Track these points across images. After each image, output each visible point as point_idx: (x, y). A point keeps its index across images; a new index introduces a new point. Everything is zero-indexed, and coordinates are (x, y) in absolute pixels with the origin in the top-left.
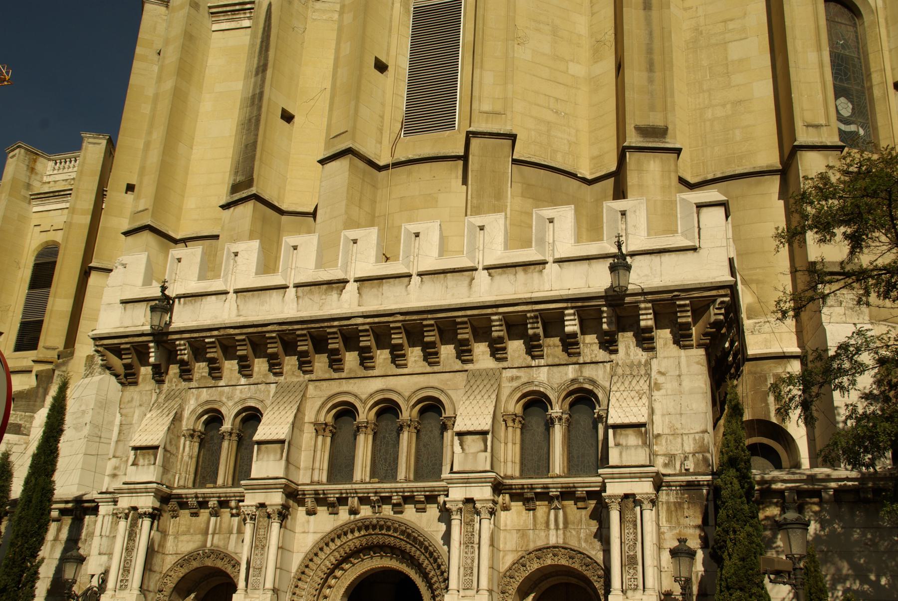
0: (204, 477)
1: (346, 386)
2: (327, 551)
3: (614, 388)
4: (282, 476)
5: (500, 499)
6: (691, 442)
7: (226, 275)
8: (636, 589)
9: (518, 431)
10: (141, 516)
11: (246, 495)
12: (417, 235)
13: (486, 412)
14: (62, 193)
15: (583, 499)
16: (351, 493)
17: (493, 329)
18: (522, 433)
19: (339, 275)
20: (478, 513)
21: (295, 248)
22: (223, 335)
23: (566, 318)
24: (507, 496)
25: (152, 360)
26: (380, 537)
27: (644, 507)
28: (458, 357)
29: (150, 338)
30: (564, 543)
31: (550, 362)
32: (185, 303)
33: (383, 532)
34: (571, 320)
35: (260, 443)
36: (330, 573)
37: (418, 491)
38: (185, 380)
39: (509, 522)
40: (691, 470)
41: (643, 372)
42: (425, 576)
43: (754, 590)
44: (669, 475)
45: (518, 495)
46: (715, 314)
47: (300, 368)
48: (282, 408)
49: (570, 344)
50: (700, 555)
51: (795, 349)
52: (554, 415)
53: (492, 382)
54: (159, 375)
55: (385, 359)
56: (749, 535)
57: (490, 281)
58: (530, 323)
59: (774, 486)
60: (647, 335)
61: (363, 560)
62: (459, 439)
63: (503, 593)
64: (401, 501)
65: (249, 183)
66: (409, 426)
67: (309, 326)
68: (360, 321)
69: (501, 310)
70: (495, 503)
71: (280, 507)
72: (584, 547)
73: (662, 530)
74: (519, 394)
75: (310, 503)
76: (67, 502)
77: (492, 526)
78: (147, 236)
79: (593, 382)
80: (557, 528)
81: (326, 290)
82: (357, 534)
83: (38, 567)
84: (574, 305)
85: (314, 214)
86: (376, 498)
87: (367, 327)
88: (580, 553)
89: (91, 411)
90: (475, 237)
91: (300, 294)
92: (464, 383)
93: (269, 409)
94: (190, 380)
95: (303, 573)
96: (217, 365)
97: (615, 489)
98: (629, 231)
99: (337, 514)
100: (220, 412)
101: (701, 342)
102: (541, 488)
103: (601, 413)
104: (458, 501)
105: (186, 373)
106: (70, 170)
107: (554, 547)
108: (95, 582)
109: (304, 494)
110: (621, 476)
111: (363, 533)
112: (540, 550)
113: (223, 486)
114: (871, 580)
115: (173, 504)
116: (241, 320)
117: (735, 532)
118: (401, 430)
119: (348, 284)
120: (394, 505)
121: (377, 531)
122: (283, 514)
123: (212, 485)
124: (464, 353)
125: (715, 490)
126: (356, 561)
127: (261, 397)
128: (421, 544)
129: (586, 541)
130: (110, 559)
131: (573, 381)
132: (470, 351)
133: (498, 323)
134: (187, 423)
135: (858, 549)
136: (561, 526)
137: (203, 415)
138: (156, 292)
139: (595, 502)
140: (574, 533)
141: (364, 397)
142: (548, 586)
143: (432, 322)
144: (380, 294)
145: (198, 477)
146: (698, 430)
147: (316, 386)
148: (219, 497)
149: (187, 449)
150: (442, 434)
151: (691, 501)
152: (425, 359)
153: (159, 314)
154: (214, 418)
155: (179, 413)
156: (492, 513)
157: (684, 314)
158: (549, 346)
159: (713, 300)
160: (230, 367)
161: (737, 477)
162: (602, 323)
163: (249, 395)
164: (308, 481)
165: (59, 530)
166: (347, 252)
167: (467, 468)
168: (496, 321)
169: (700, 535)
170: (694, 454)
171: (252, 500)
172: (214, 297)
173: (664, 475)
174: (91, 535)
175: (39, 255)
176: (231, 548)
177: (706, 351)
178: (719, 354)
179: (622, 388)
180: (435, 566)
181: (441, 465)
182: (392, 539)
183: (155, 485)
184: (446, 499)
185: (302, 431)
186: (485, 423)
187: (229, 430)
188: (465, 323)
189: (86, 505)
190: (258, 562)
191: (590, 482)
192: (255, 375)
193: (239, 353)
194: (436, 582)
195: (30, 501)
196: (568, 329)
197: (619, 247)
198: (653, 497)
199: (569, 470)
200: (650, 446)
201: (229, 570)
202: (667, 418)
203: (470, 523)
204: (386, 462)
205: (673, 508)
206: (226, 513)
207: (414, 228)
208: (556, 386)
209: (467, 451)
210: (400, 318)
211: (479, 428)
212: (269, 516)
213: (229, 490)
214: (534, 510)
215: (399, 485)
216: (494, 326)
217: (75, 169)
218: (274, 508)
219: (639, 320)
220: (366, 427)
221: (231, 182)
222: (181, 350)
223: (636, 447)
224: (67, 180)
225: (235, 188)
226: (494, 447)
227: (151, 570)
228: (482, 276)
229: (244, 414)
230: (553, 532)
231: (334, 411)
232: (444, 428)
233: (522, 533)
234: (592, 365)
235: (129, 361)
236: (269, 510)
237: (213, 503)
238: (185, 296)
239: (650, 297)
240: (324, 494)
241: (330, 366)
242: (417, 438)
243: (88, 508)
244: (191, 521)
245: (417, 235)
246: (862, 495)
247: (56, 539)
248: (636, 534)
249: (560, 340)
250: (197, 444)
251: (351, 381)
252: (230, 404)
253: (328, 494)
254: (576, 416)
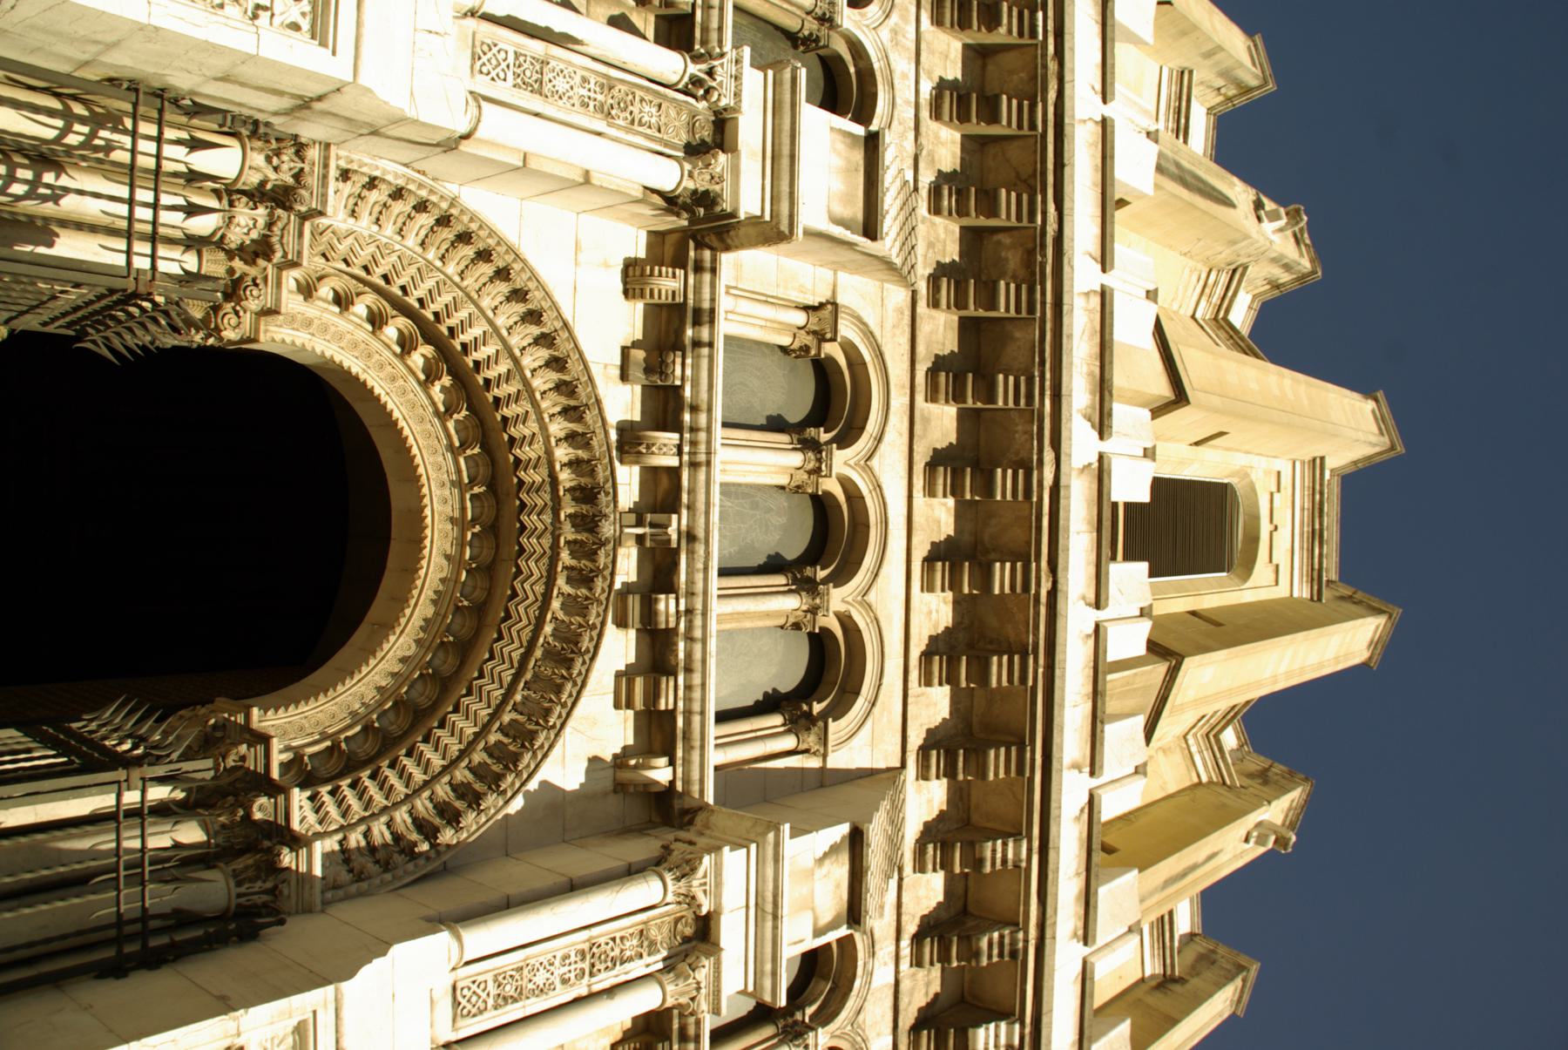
16: (693, 443)
22: (1045, 67)
31: (905, 985)
33: (565, 557)
34: (997, 1036)
37: (688, 688)
57: (1074, 816)
58: (1002, 937)
71: (727, 206)
75: (668, 284)
84: (1027, 1039)
86: (674, 537)
99: (624, 377)
104: (718, 896)
109: (698, 268)
111: (565, 477)
119: (1096, 434)
121: (568, 533)
133: (1010, 855)
147: (902, 313)
163: (898, 101)
168: (1017, 853)
182: (539, 588)
190: (561, 85)
216: (1005, 844)
229: (852, 70)
240: (697, 344)
252: (885, 33)
253: (697, 358)
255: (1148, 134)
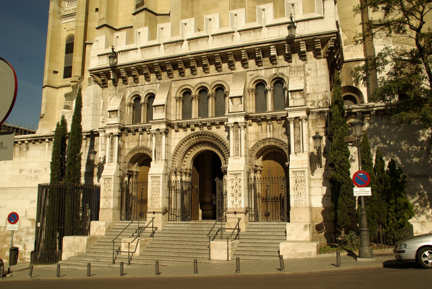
0: (136, 121)
1: (186, 82)
2: (184, 145)
3: (291, 76)
4: (164, 118)
5: (248, 122)
6: (321, 95)
7: (136, 41)
8: (300, 152)
9: (254, 96)
10: (114, 136)
11: (152, 126)
12: (210, 20)
13: (241, 89)
14: (73, 14)
15: (280, 120)
17: (242, 56)
18: (256, 96)
19: (181, 38)
20: (240, 127)
21: (162, 29)
23: (271, 49)
24: (251, 121)
25: (112, 77)
26: (203, 138)
27: (303, 121)
28: (229, 68)
29: (110, 69)
30: (273, 137)
31: (265, 67)
32: (122, 54)
33: (204, 137)
34: (273, 50)
35: (155, 106)
36: (186, 153)
38: (125, 84)
39: (252, 130)
40: (321, 107)
41: (302, 69)
42: (221, 152)
43: (344, 149)
44: (312, 109)
45: (255, 120)
46: (330, 44)
47: (168, 76)
48: (162, 92)
49: (273, 60)
50: (324, 138)
51: (362, 57)
52: (268, 88)
53: (243, 77)
54: (115, 83)
55: (201, 71)
56: (342, 129)
59: (353, 111)
60: (303, 54)
61: (198, 147)
62: (231, 100)
63: (250, 156)
64: (210, 125)
65: (142, 3)
66: (212, 96)
67: (170, 59)
68: (190, 56)
69: (245, 48)
70: (246, 123)
71: (165, 130)
72: (281, 138)
73: (310, 130)
74: (254, 81)
75: (176, 127)
76: (88, 133)
77: (245, 132)
78: (105, 29)
79: (282, 74)
80: (270, 131)
81: (176, 45)
82: (195, 138)
83: (81, 156)
84: (274, 44)
85: (169, 15)
87: (193, 58)
88: (279, 140)
89: (92, 99)
90: (233, 19)
91: (166, 47)
92: (232, 78)
93: (158, 93)
94: (127, 84)
95: (176, 153)
96: (136, 77)
97: (291, 115)
98: (295, 12)
100: (139, 96)
101: (325, 56)
102: (264, 117)
103: (286, 86)
105: (125, 81)
106: (74, 5)
107: (269, 139)
108: (102, 160)
109: (174, 125)
110: (294, 110)
111: (197, 137)
112: (264, 140)
113: (143, 123)
114: (387, 143)
115: (126, 131)
116: (144, 59)
117: (337, 129)
118: (209, 98)
119: (184, 42)
120: (208, 126)
121: (202, 136)
122: (166, 132)
123: (139, 123)
124: (231, 66)
125: (330, 114)
126: (195, 148)
127: (154, 89)
128: (219, 140)
129: (281, 135)
130: (106, 152)
131: (275, 74)
132: (234, 65)
133: (244, 53)
134: (128, 101)
135: (383, 132)
136: (272, 130)
137: (133, 97)
138: (110, 51)
139: (284, 121)
140: (277, 133)
141: (194, 86)
142: (268, 153)
143: (218, 55)
144: (197, 45)
145: (134, 121)
146: (324, 91)
148: (142, 127)
149: (129, 110)
150: (225, 98)
151: (321, 118)
152: (216, 69)
153: (112, 59)
154: (137, 98)
155: (124, 97)
156: (245, 127)
157: (318, 45)
158: (265, 61)
159: (329, 39)
160: (142, 78)
161: (338, 108)
162: (285, 51)
163: (150, 88)
164: (175, 120)
165: (87, 143)
166: (183, 29)
167: (235, 111)
169: (324, 131)
170: (322, 100)
171: (154, 128)
172: (132, 51)
173: (311, 109)
174: (98, 144)
175: (67, 40)
176: (149, 146)
177: (327, 59)
178: (332, 61)
179: (294, 76)
180: (225, 148)
181: (225, 110)
183: (118, 125)
184: (227, 123)
185: (171, 101)
186: (241, 93)
187: (144, 102)
188: (231, 54)
189: (95, 133)
190: (159, 150)
191: (282, 113)
192: (151, 80)
193: (144, 72)
194: (225, 154)
195: (74, 133)
196: (272, 54)
197: (291, 19)
198: (306, 117)
199: (274, 109)
200: (305, 98)
201: (149, 154)
202: (312, 87)
203: (237, 131)
204: (204, 110)
205: (314, 121)
206: (145, 133)
207: (209, 17)
208: (268, 77)
209: (234, 104)
210: (205, 54)
211: (238, 95)
212: (161, 133)
213: (145, 125)
214: (261, 125)
215: (209, 119)
217: (76, 4)
218: (163, 130)
219: (300, 49)
220: (195, 98)
221: (136, 4)
222: (122, 73)
223: (300, 99)
224: (73, 9)
225: (137, 6)
226: (245, 102)
227: (120, 155)
228: (237, 34)
230: (268, 133)
231: (183, 92)
232: (225, 96)
233: (257, 134)
234: (282, 68)
235: (103, 78)
236: (161, 131)
237: (140, 130)
238: (122, 51)
239: (304, 39)
240: (181, 124)
241: (180, 75)
242: (215, 100)
243: (95, 134)
244: (133, 137)
245: (210, 20)
246: (386, 112)
247: (86, 146)
248: (300, 132)
249: (269, 59)
250: (132, 108)
251: (188, 80)
252: (143, 92)
254: (276, 88)
255: (139, 33)
